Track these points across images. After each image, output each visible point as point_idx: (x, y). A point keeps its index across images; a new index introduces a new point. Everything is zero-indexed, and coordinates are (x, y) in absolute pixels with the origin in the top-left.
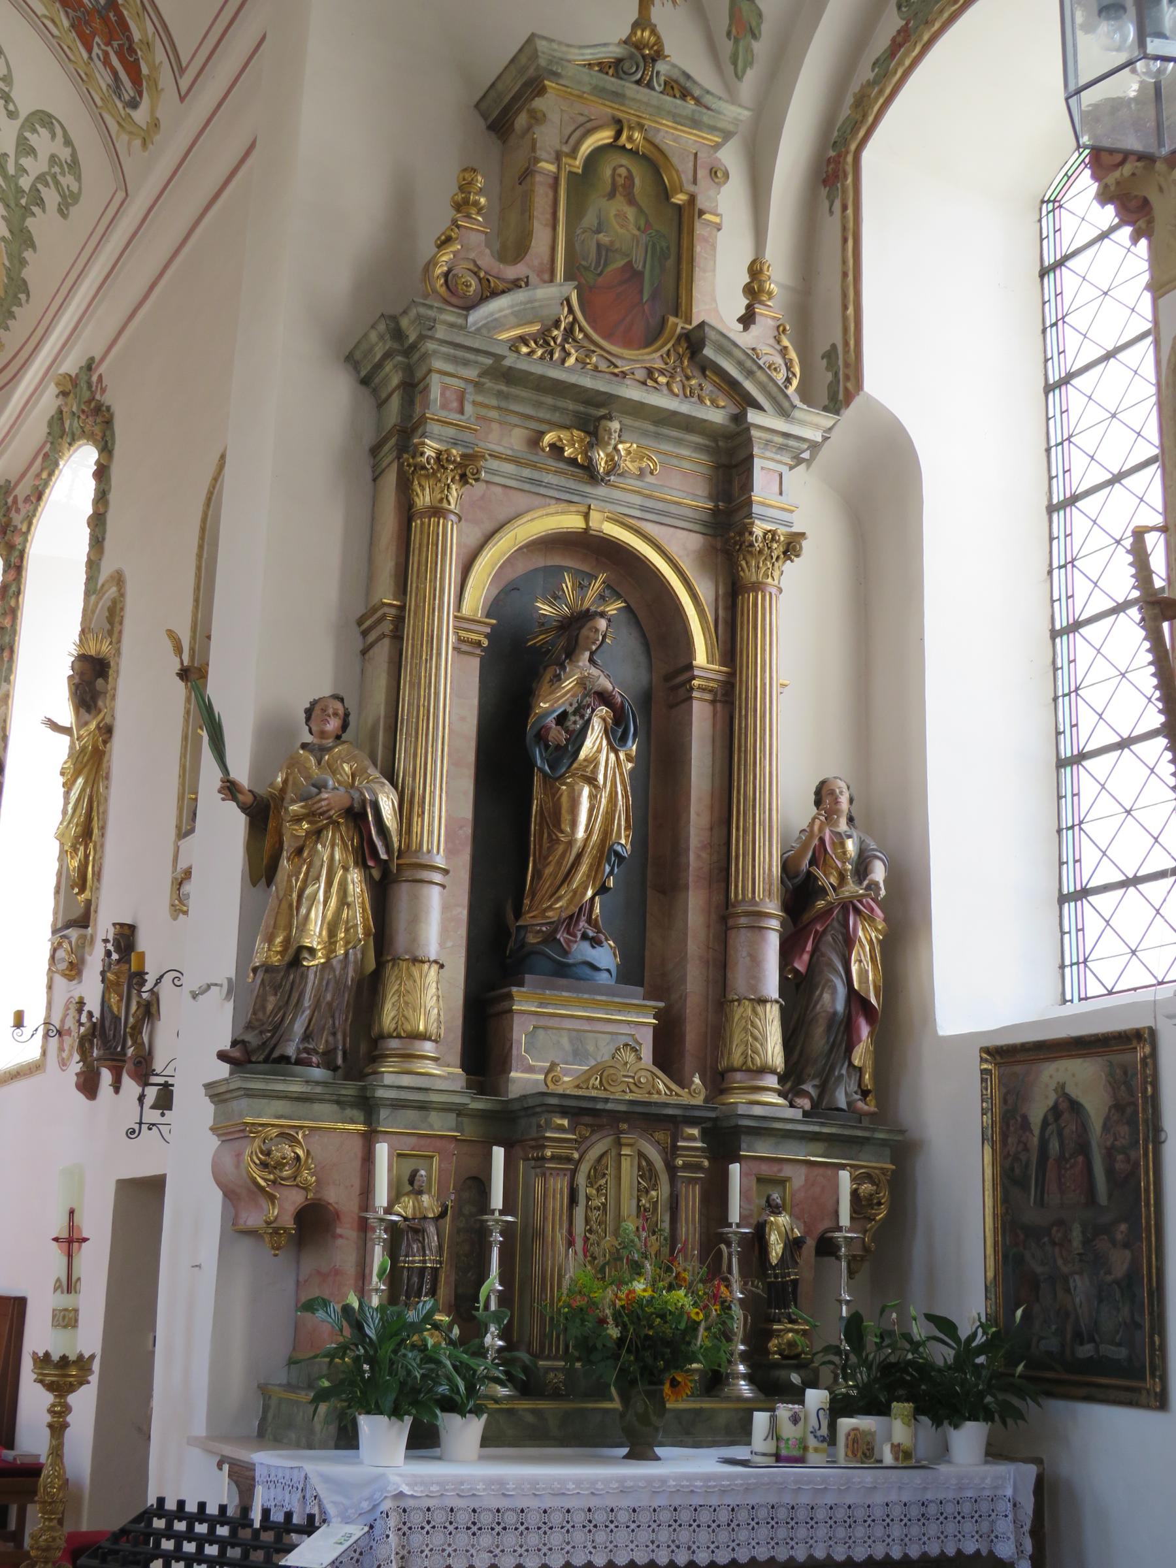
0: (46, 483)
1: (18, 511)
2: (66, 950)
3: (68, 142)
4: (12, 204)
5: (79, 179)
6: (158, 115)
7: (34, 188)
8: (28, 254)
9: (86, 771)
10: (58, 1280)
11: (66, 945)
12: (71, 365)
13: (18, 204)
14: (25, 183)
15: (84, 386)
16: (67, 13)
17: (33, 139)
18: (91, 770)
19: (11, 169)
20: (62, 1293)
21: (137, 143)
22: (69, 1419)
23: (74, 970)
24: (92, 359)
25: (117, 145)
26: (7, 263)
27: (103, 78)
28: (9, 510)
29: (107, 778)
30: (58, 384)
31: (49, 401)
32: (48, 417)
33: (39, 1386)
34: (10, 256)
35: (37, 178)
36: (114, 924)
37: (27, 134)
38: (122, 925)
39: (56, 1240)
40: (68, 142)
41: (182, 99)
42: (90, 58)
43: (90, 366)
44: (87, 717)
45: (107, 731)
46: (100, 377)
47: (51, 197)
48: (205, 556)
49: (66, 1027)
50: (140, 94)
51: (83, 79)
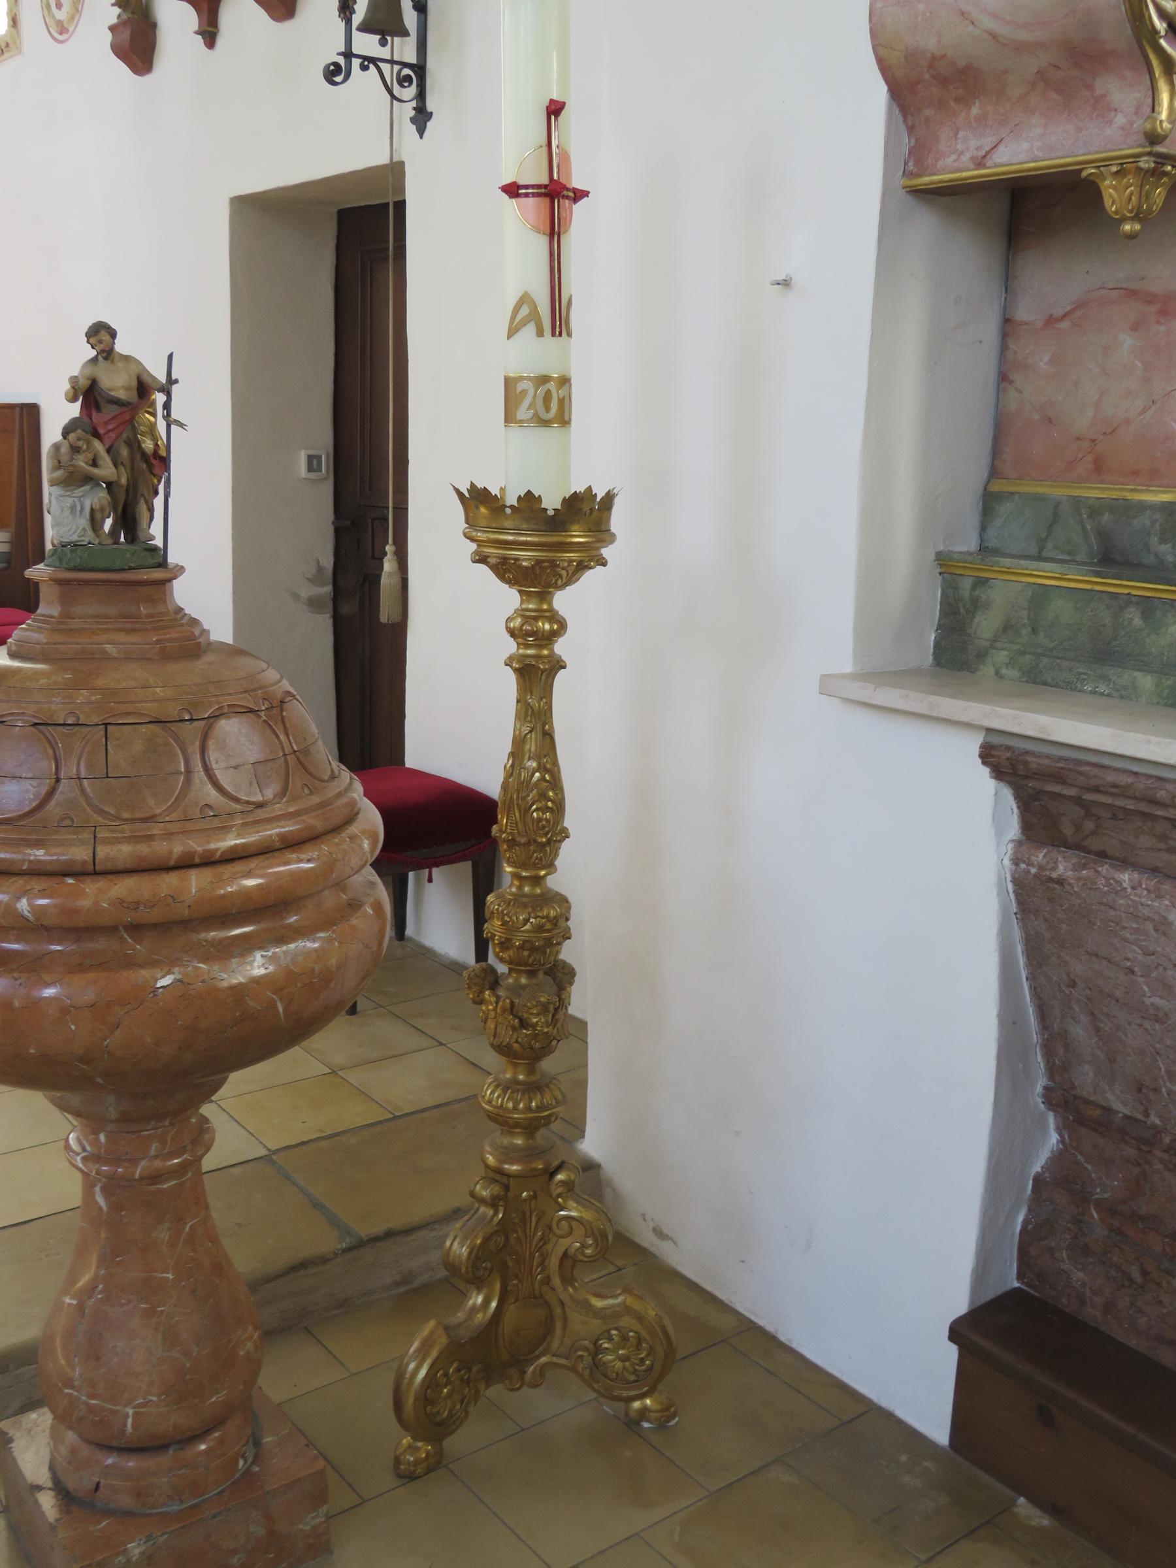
10: (525, 299)
20: (540, 333)
22: (561, 647)
33: (483, 568)
39: (512, 190)
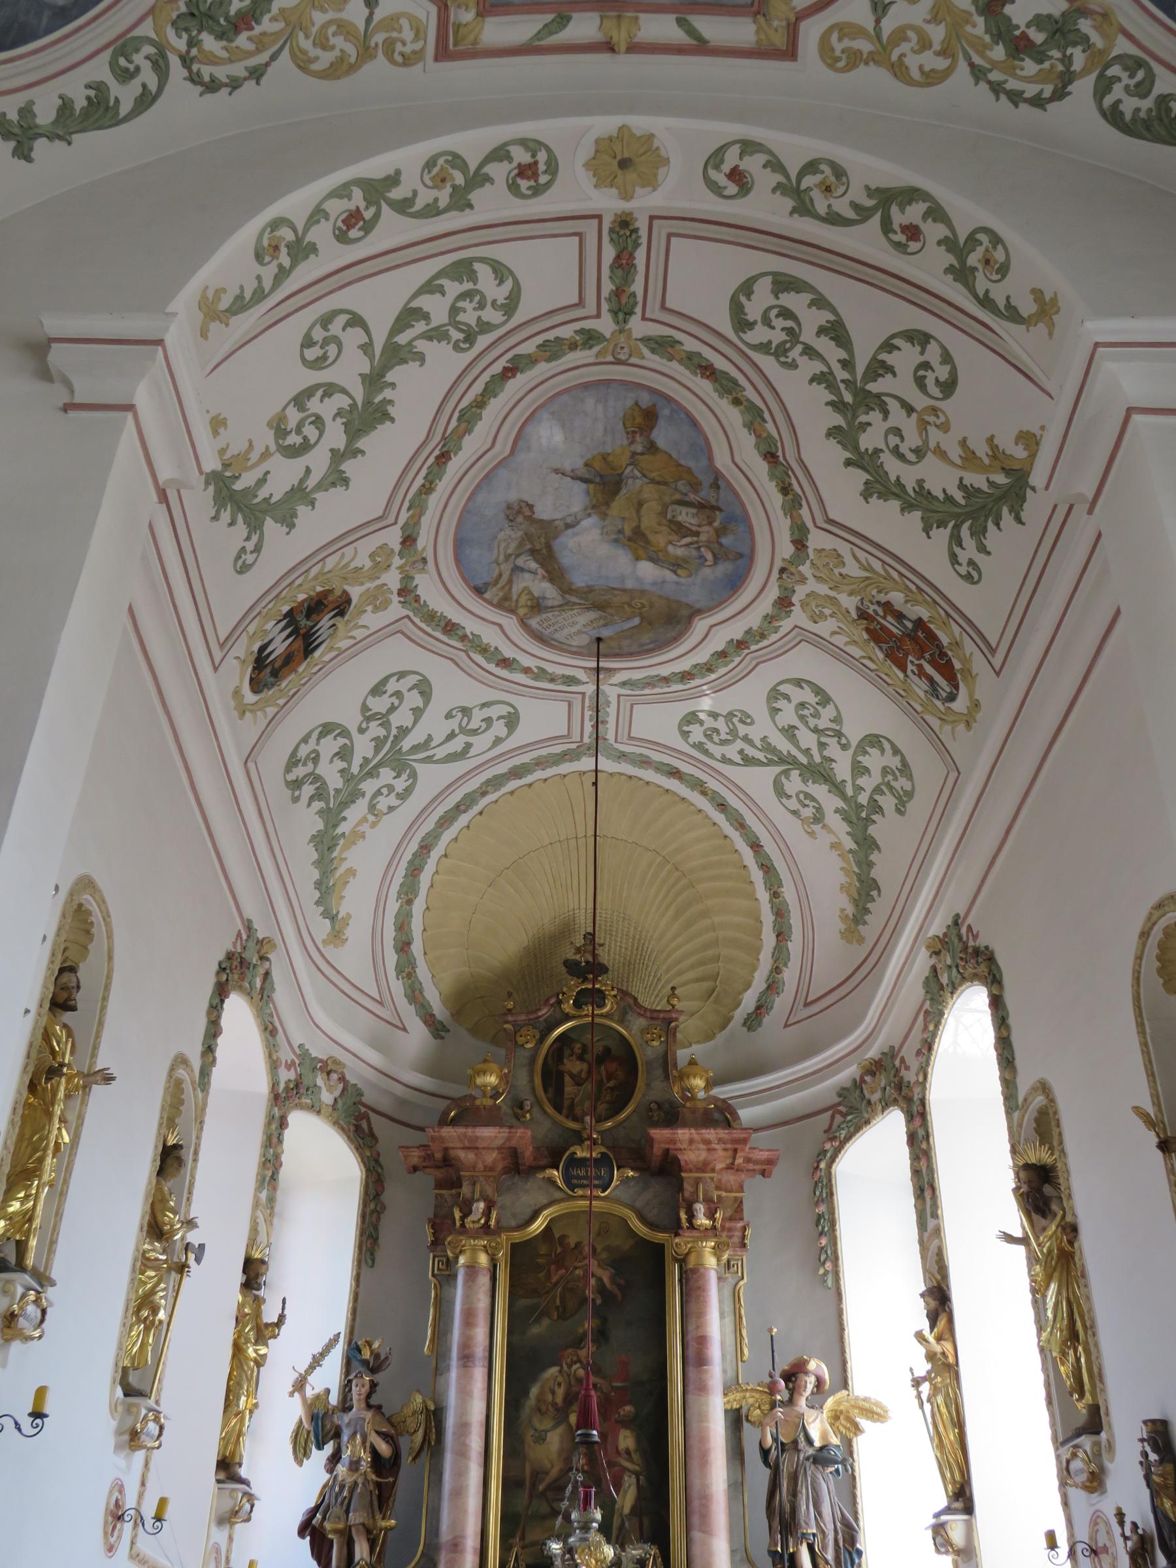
0: (934, 1035)
1: (907, 1068)
2: (1083, 1460)
3: (896, 751)
4: (855, 820)
5: (910, 778)
6: (976, 696)
7: (872, 800)
8: (874, 857)
9: (1056, 1275)
11: (1081, 1454)
12: (937, 928)
13: (859, 818)
14: (863, 799)
15: (956, 941)
16: (881, 648)
17: (865, 760)
18: (1062, 1272)
19: (850, 792)
21: (961, 727)
23: (1096, 1481)
24: (957, 915)
25: (941, 737)
26: (857, 870)
27: (920, 687)
28: (898, 1071)
29: (1083, 1276)
30: (928, 947)
31: (923, 962)
32: (923, 979)
34: (859, 864)
35: (874, 790)
36: (1145, 1422)
37: (860, 758)
38: (1153, 1421)
40: (896, 751)
41: (998, 674)
42: (906, 676)
43: (956, 922)
44: (1043, 1222)
45: (1072, 1230)
46: (969, 928)
47: (888, 802)
48: (1148, 1031)
49: (1100, 1544)
50: (957, 687)
51: (901, 697)
